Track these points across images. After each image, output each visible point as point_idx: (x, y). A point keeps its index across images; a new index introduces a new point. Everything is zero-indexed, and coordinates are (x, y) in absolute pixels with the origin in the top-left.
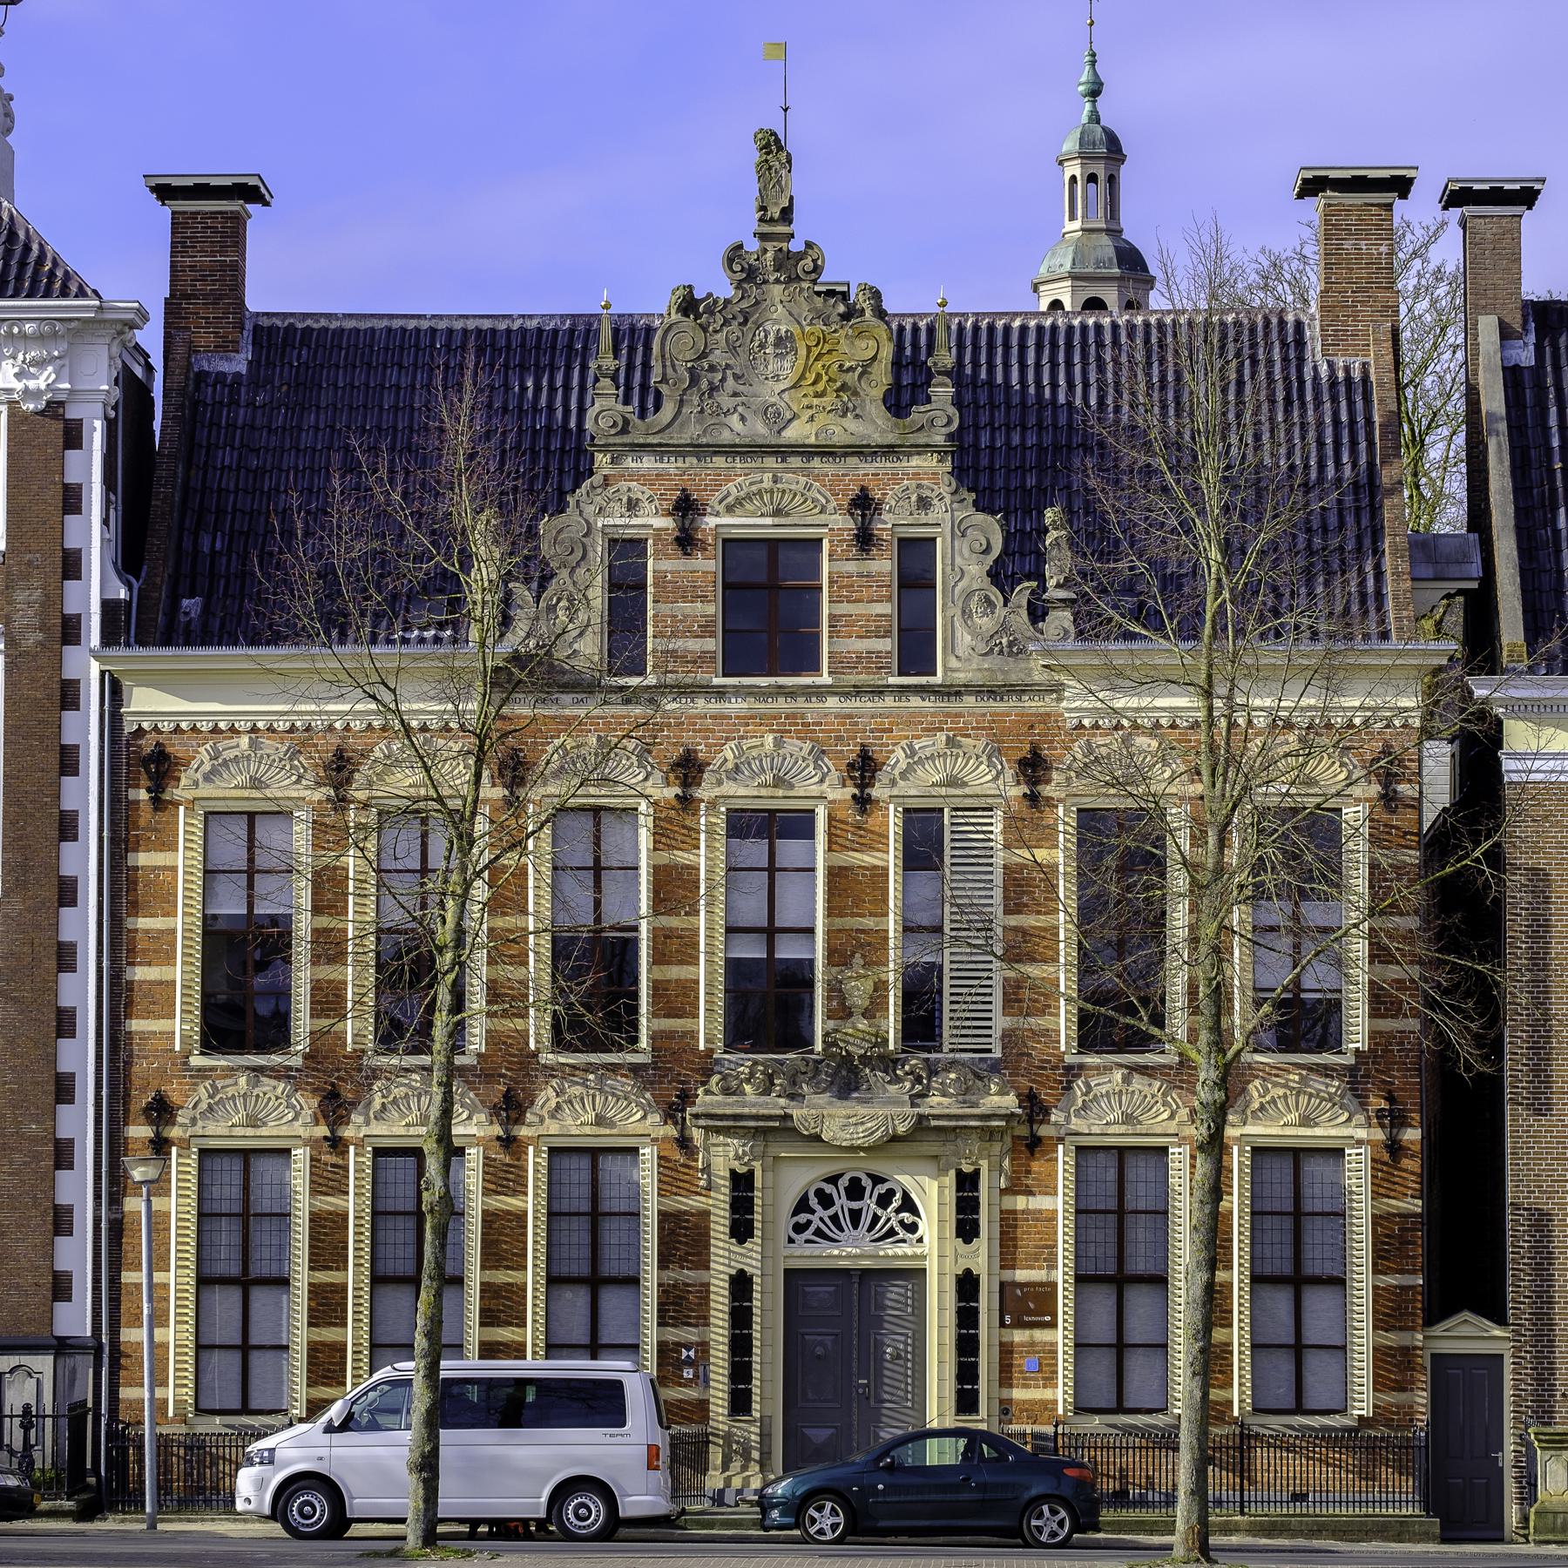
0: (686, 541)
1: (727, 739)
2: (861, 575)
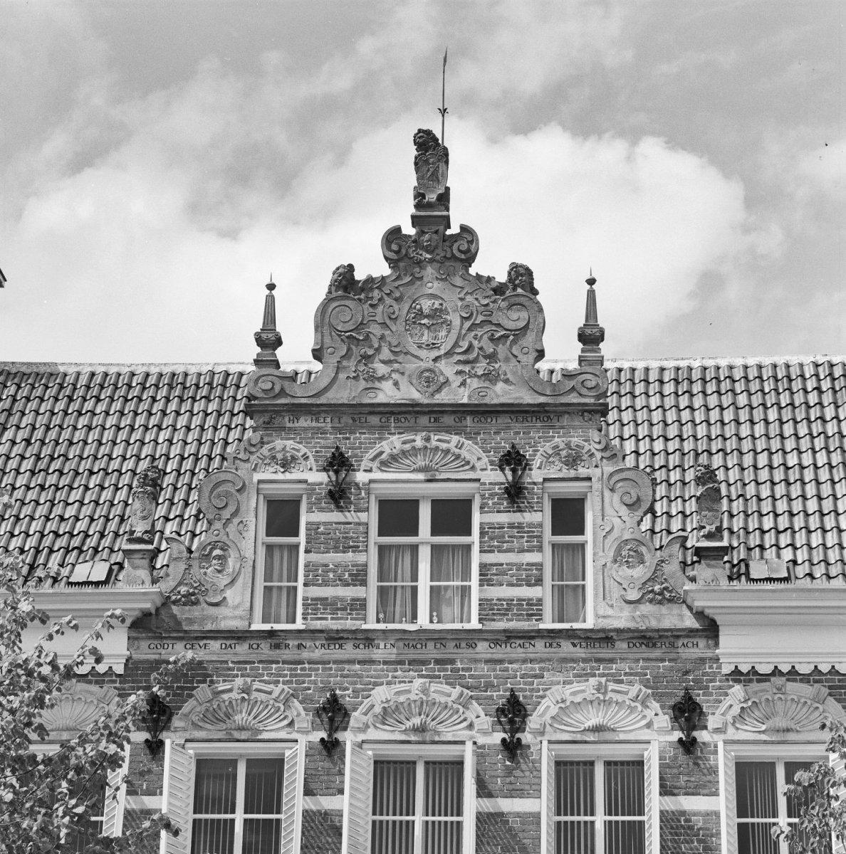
0: (338, 496)
1: (376, 684)
2: (511, 526)
